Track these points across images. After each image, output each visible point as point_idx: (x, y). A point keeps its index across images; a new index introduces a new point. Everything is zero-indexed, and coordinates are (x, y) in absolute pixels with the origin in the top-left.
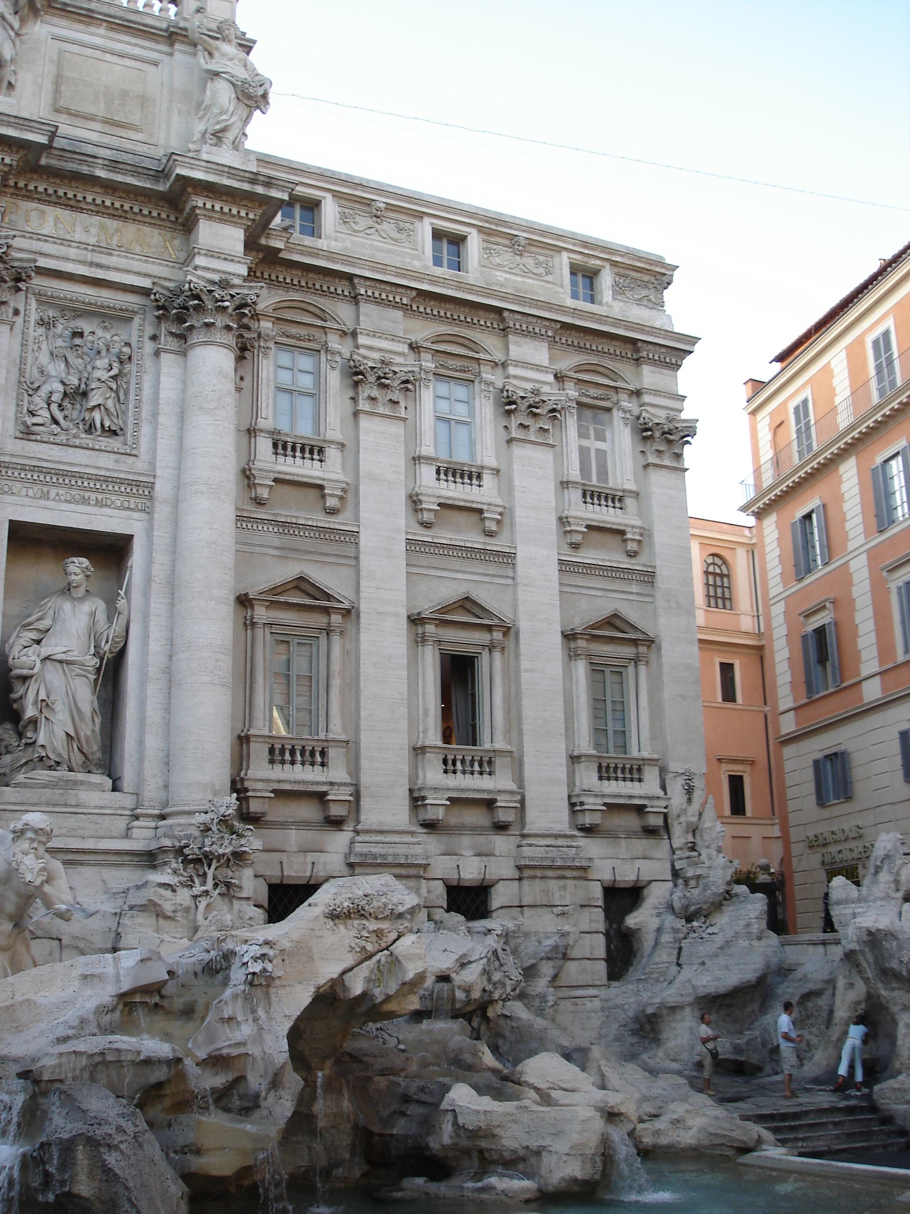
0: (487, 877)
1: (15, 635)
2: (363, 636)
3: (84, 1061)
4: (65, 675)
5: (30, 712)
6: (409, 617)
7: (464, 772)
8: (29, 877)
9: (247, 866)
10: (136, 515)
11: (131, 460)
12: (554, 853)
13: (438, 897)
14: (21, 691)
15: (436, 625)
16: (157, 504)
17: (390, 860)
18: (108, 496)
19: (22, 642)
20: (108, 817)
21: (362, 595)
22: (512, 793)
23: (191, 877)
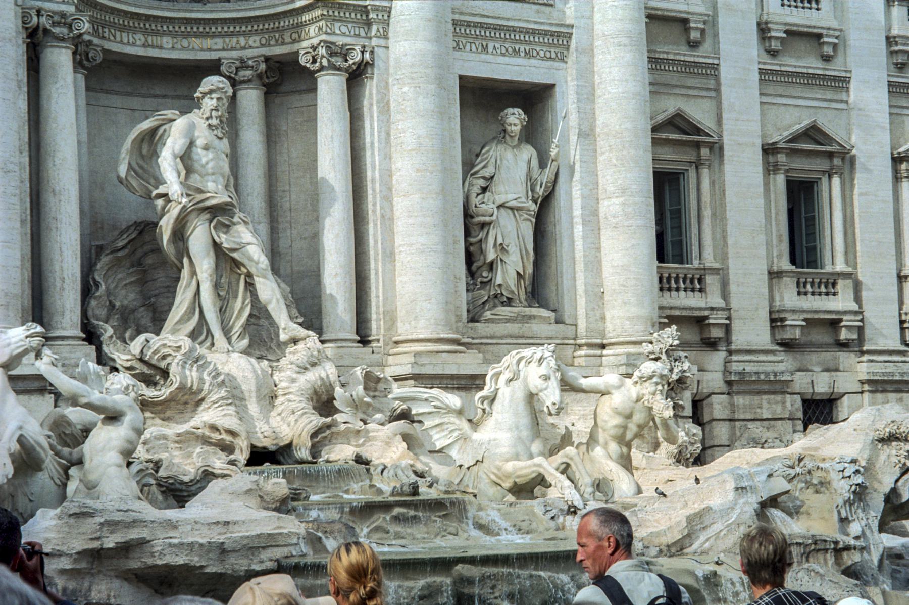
0: (836, 390)
2: (728, 167)
4: (516, 220)
5: (491, 255)
6: (763, 146)
7: (813, 294)
9: (686, 388)
11: (548, 9)
12: (891, 368)
13: (797, 410)
14: (482, 235)
15: (787, 155)
17: (762, 377)
18: (534, 47)
19: (476, 190)
21: (725, 127)
22: (856, 313)
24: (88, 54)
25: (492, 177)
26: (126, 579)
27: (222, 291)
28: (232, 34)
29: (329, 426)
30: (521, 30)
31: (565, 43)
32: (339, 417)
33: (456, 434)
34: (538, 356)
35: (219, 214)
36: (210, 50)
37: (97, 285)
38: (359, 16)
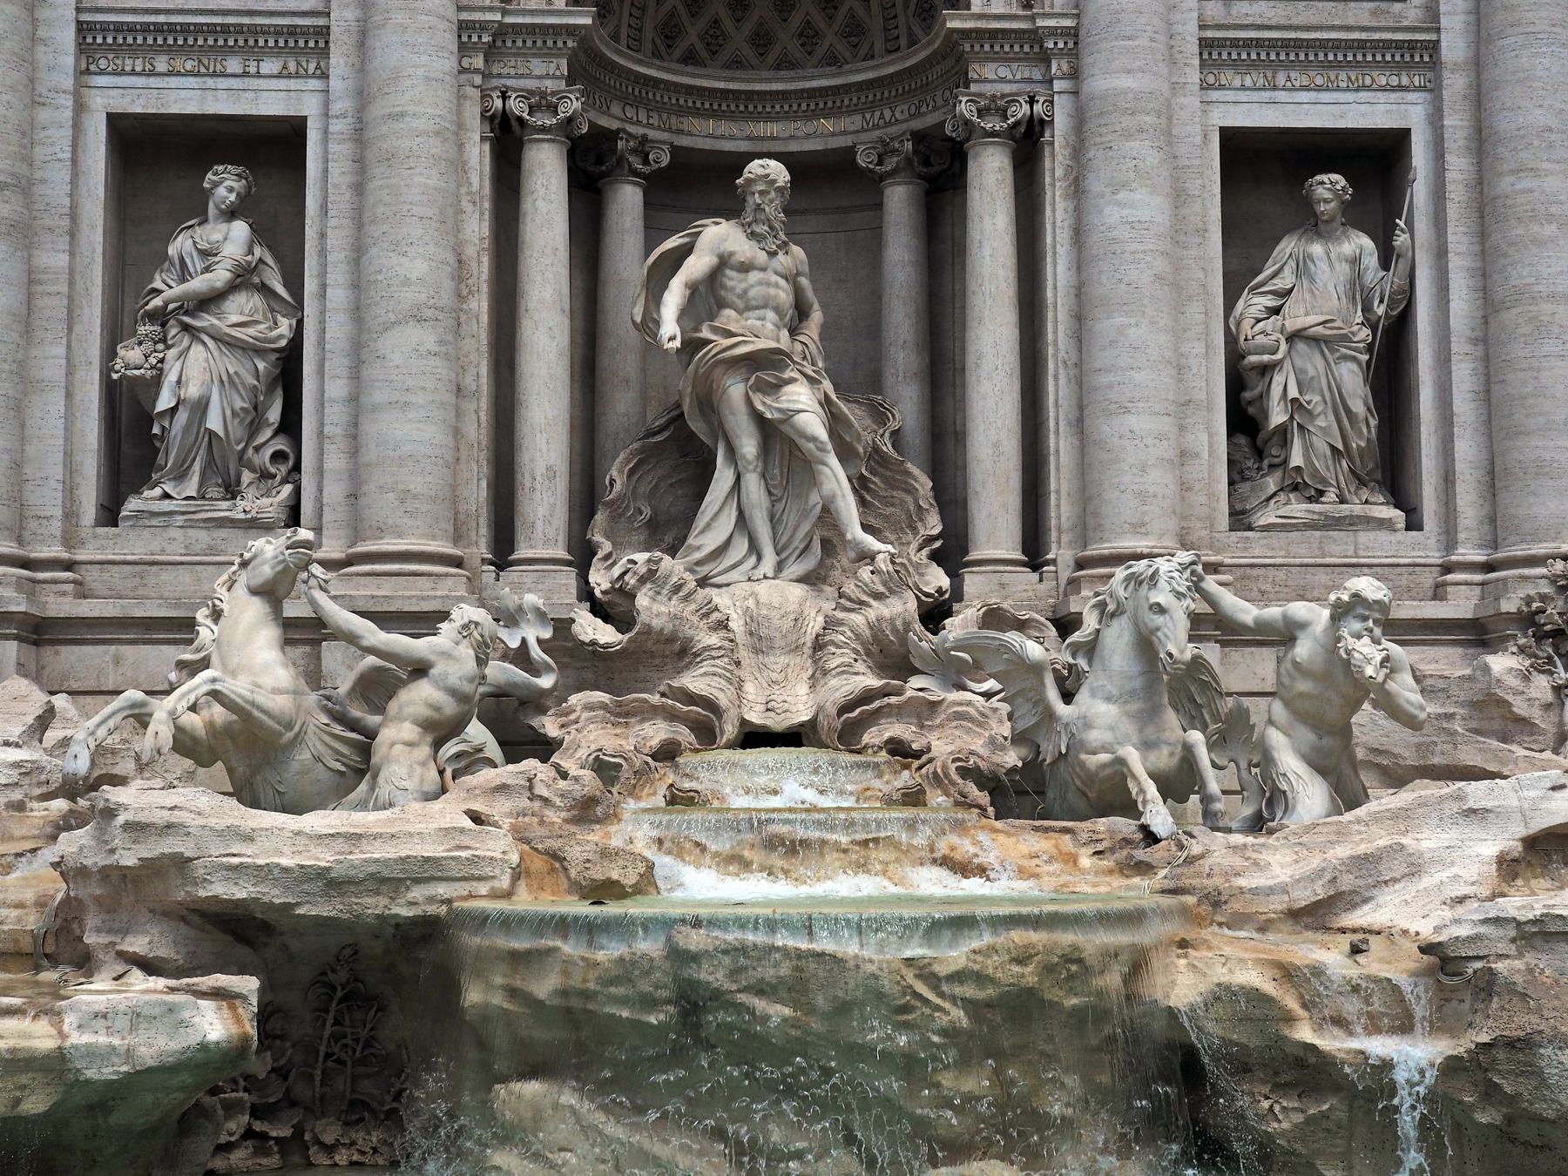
1: (1240, 305)
3: (1513, 933)
5: (1277, 417)
8: (1369, 671)
10: (1412, 96)
16: (1446, 74)
20: (1404, 569)
23: (1550, 658)
24: (647, 155)
25: (1291, 290)
26: (183, 919)
27: (775, 487)
28: (872, 107)
29: (884, 692)
30: (1337, 45)
31: (1426, 59)
32: (916, 682)
33: (1040, 709)
34: (1151, 571)
35: (765, 367)
36: (845, 133)
37: (612, 485)
38: (1027, 48)
